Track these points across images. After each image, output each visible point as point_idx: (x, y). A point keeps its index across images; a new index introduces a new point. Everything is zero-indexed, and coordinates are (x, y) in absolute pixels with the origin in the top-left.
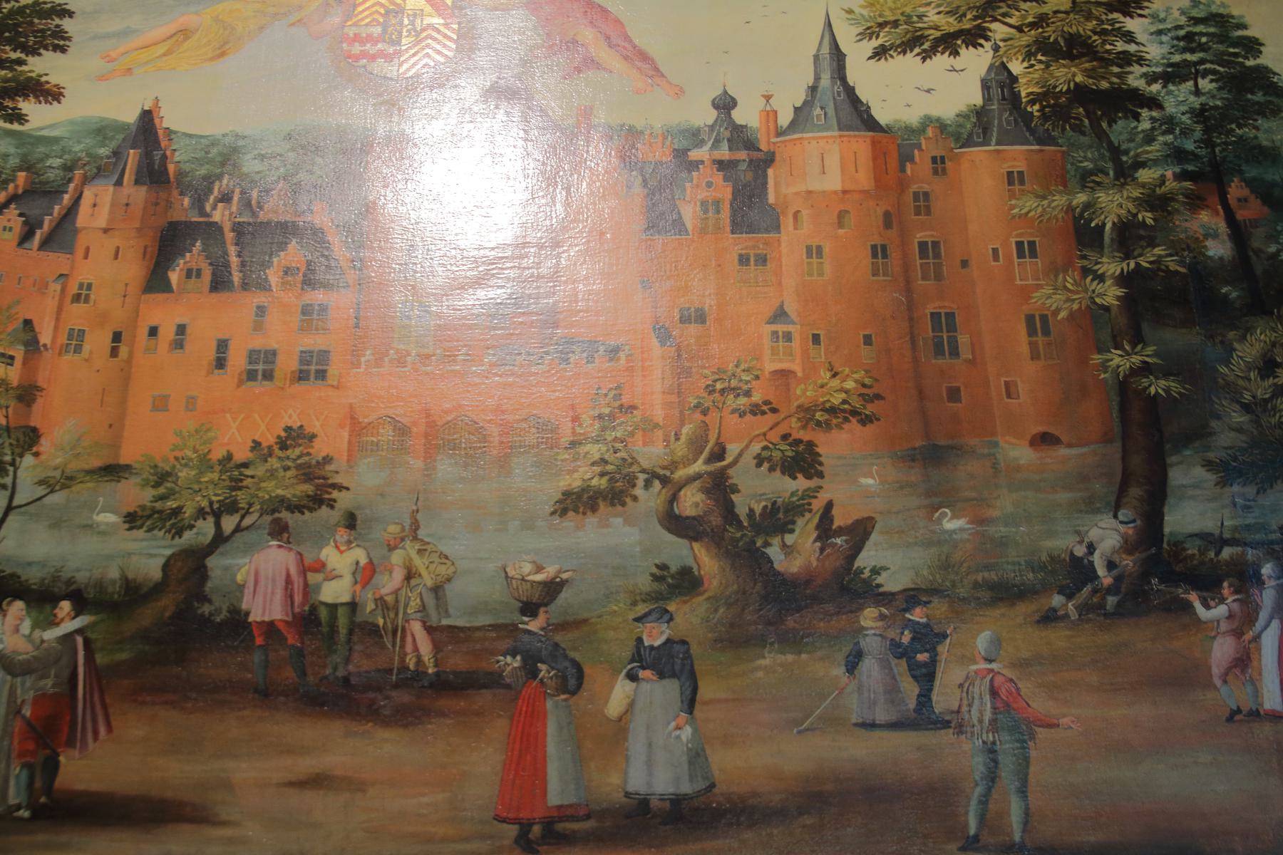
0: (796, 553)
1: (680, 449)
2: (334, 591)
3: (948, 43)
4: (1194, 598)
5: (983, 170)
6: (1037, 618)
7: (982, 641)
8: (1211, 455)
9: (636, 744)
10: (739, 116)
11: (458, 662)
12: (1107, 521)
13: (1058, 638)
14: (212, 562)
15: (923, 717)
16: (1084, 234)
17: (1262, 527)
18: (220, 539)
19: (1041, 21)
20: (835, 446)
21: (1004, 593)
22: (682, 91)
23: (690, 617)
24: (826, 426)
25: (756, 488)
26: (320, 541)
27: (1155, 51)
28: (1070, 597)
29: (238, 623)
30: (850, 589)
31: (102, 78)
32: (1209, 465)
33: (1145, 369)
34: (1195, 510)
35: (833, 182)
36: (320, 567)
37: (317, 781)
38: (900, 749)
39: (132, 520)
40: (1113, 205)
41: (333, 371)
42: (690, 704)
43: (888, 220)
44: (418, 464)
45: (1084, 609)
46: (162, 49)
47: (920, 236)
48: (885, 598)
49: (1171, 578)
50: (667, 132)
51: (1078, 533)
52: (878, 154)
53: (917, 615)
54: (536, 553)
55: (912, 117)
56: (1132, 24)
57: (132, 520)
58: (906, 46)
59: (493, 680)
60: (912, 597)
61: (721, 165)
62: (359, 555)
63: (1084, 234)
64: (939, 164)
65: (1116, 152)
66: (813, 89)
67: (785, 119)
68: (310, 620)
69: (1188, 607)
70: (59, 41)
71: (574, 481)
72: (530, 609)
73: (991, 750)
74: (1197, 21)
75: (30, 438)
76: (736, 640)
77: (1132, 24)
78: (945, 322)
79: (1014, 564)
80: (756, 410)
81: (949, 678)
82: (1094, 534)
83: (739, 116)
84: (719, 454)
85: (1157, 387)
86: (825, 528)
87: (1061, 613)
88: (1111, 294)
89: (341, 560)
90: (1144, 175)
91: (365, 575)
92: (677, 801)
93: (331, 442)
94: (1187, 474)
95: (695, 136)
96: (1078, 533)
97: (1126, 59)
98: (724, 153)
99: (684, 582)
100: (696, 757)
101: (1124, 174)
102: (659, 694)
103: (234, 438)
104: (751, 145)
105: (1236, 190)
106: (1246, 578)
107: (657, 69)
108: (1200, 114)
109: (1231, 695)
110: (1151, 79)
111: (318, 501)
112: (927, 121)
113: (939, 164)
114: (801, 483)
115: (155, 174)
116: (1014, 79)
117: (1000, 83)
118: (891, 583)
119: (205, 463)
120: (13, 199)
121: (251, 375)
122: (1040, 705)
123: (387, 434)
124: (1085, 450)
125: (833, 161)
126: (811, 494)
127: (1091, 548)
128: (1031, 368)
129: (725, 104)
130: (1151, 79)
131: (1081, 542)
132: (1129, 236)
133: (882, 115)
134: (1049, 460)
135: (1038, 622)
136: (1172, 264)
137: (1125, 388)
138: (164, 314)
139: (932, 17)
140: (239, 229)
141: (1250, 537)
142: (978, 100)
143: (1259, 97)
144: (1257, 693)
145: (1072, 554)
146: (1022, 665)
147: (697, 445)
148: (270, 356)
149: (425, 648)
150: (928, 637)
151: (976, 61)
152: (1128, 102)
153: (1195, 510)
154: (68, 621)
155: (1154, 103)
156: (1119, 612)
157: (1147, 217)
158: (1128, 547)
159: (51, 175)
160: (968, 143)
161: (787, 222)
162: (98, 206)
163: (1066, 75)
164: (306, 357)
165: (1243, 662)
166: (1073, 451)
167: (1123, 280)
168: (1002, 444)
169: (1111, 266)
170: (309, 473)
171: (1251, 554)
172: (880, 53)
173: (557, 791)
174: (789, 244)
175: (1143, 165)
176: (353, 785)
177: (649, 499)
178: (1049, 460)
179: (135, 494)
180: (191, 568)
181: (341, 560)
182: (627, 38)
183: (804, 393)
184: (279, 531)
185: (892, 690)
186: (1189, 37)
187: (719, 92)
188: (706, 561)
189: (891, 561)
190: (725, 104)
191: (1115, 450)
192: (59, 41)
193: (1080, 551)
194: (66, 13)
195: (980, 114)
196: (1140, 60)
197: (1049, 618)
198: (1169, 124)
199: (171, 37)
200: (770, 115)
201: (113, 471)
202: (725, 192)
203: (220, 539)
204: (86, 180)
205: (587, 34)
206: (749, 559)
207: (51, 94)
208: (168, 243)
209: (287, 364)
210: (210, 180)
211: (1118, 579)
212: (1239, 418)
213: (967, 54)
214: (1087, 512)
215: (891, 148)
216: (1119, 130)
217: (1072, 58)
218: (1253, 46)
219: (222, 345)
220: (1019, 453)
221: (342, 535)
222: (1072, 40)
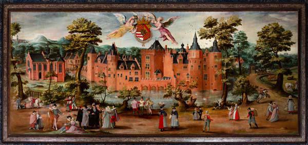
0: (188, 102)
1: (177, 90)
2: (141, 105)
3: (210, 37)
5: (212, 55)
7: (206, 112)
9: (172, 121)
10: (184, 47)
11: (154, 113)
12: (221, 99)
14: (128, 102)
15: (200, 119)
16: (222, 64)
18: (129, 99)
19: (221, 33)
20: (193, 90)
21: (209, 107)
23: (177, 108)
24: (192, 88)
25: (185, 95)
26: (139, 99)
27: (234, 39)
29: (131, 108)
30: (194, 106)
31: (107, 39)
32: (232, 93)
33: (227, 82)
34: (229, 99)
35: (195, 57)
36: (139, 103)
37: (141, 125)
38: (198, 123)
39: (119, 97)
40: (226, 60)
41: (139, 80)
42: (177, 118)
43: (201, 62)
44: (149, 91)
46: (114, 35)
47: (204, 64)
48: (197, 107)
50: (176, 49)
52: (200, 53)
53: (200, 109)
54: (162, 101)
55: (204, 48)
56: (232, 35)
57: (119, 97)
58: (204, 37)
59: (158, 115)
60: (200, 107)
61: (182, 54)
62: (143, 101)
63: (222, 64)
64: (207, 54)
65: (228, 53)
66: (193, 43)
67: (190, 48)
68: (139, 108)
70: (100, 33)
71: (166, 94)
72: (161, 107)
73: (206, 123)
74: (240, 34)
75: (106, 87)
76: (182, 111)
77: (232, 35)
78: (206, 76)
80: (185, 86)
81: (203, 116)
83: (184, 47)
84: (181, 91)
85: (228, 84)
86: (192, 99)
88: (224, 72)
89: (142, 102)
90: (231, 57)
91: (144, 104)
92: (176, 127)
93: (139, 89)
94: (230, 94)
95: (179, 50)
97: (231, 40)
98: (182, 53)
99: (177, 105)
100: (178, 123)
101: (228, 56)
102: (174, 116)
103: (129, 88)
104: (186, 52)
105: (241, 59)
106: (234, 105)
108: (238, 48)
109: (230, 118)
110: (233, 43)
111: (139, 95)
112: (206, 48)
113: (207, 54)
114: (189, 94)
115: (115, 53)
116: (217, 42)
117: (215, 43)
118: (198, 105)
119: (126, 91)
120: (99, 56)
121: (130, 80)
122: (211, 118)
123: (145, 88)
125: (195, 54)
126: (190, 95)
128: (215, 81)
129: (183, 45)
130: (233, 43)
132: (228, 65)
133: (201, 47)
136: (232, 69)
137: (224, 84)
138: (119, 72)
139: (208, 33)
140: (126, 61)
142: (212, 45)
143: (245, 46)
146: (210, 114)
147: (179, 90)
148: (132, 78)
149: (151, 111)
150: (201, 111)
151: (213, 40)
152: (230, 46)
154: (114, 108)
155: (233, 46)
157: (230, 62)
158: (222, 102)
159: (103, 53)
160: (211, 51)
161: (189, 62)
162: (110, 57)
163: (224, 42)
164: (136, 78)
165: (232, 114)
167: (226, 70)
169: (225, 69)
170: (138, 92)
172: (201, 38)
173: (164, 126)
174: (189, 65)
175: (230, 55)
176: (145, 125)
177: (173, 96)
179: (119, 94)
180: (126, 102)
181: (142, 102)
183: (190, 84)
184: (135, 99)
185: (197, 117)
186: (239, 36)
188: (179, 103)
189: (198, 103)
190: (183, 45)
191: (222, 91)
192: (100, 33)
194: (100, 29)
195: (212, 47)
196: (232, 40)
197: (214, 109)
198: (234, 49)
200: (188, 47)
201: (116, 91)
202: (182, 58)
203: (129, 99)
204: (107, 54)
205: (166, 35)
206: (184, 102)
207: (101, 41)
208: (119, 63)
209: (134, 79)
210: (122, 55)
212: (236, 88)
213: (212, 38)
215: (202, 52)
216: (229, 50)
217: (224, 39)
218: (246, 38)
219: (126, 76)
220: (212, 91)
221: (142, 99)
222: (225, 37)
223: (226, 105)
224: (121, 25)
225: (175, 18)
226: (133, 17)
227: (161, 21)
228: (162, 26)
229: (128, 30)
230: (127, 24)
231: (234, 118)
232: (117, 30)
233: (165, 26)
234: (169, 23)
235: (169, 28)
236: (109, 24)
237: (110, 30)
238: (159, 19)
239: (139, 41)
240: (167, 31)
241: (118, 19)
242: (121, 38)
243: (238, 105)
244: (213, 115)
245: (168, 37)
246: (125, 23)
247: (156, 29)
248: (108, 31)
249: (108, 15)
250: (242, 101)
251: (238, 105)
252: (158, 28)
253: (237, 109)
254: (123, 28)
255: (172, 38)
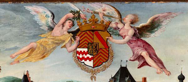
22: (170, 73)
31: (11, 64)
46: (27, 54)
107: (163, 66)
182: (156, 56)
187: (180, 74)
199: (30, 49)
205: (144, 53)
224: (43, 32)
225: (165, 17)
226: (71, 15)
227: (132, 22)
228: (134, 35)
229: (58, 44)
230: (57, 31)
232: (34, 44)
233: (141, 34)
234: (152, 27)
235: (150, 39)
236: (16, 30)
237: (17, 44)
238: (128, 19)
239: (85, 68)
240: (147, 47)
241: (36, 18)
242: (42, 61)
245: (149, 60)
246: (51, 29)
247: (122, 41)
248: (12, 46)
249: (14, 10)
252: (127, 38)
254: (47, 39)
255: (159, 62)
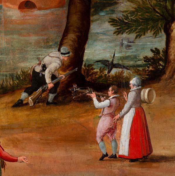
4: (93, 96)
6: (12, 105)
8: (114, 16)
12: (54, 53)
13: (21, 114)
17: (135, 58)
28: (30, 94)
32: (113, 22)
34: (97, 51)
45: (37, 101)
49: (83, 84)
51: (38, 59)
69: (90, 100)
79: (3, 75)
82: (46, 60)
87: (24, 102)
94: (101, 27)
96: (38, 59)
106: (122, 85)
109: (103, 147)
124: (48, 11)
127: (44, 67)
131: (39, 64)
134: (28, 18)
135: (13, 106)
141: (127, 63)
144: (117, 147)
145: (34, 71)
153: (102, 47)
156: (56, 103)
158: (64, 67)
165: (112, 130)
166: (42, 12)
168: (4, 7)
171: (126, 73)
178: (28, 18)
191: (63, 12)
193: (38, 69)
197: (20, 104)
211: (56, 85)
214: (44, 48)
223: (81, 82)
231: (124, 149)
243: (144, 84)
244: (19, 135)
250: (166, 60)
251: (144, 84)
253: (138, 102)
